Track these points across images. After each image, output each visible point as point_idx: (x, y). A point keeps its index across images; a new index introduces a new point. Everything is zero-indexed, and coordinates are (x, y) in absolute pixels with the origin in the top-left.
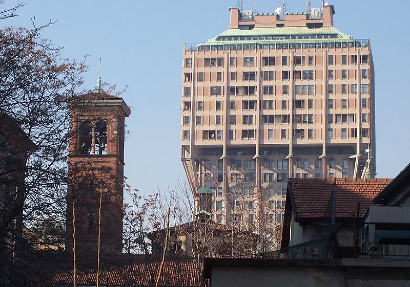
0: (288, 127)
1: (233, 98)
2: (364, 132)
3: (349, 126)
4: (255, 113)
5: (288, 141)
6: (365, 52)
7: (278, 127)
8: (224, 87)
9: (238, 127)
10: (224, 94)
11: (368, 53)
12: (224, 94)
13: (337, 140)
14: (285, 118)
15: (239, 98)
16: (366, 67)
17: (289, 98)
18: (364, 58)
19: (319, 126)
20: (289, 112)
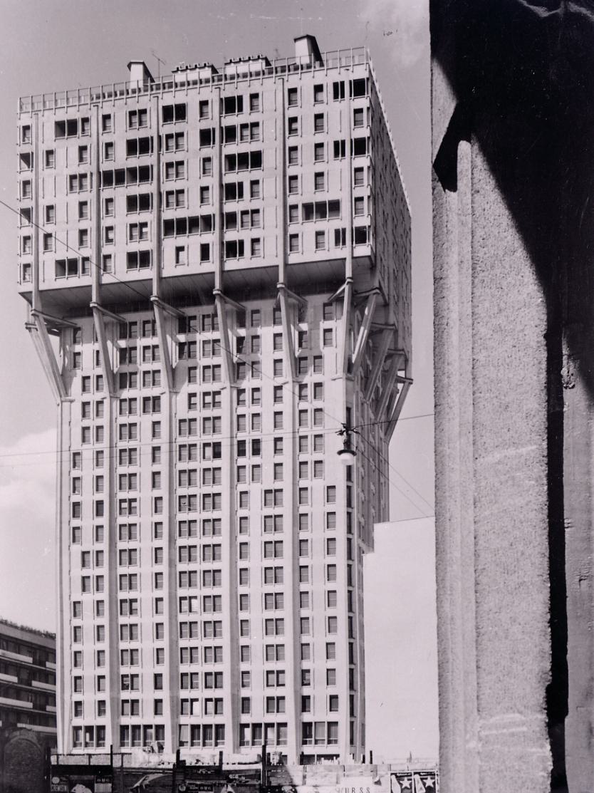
0: (211, 238)
1: (107, 193)
2: (360, 236)
3: (329, 225)
4: (148, 216)
5: (212, 266)
6: (360, 73)
7: (193, 242)
8: (91, 174)
9: (120, 248)
10: (91, 188)
11: (365, 75)
12: (91, 188)
13: (306, 253)
14: (207, 222)
15: (120, 194)
16: (363, 102)
17: (212, 181)
18: (359, 87)
19: (270, 229)
20: (211, 209)
